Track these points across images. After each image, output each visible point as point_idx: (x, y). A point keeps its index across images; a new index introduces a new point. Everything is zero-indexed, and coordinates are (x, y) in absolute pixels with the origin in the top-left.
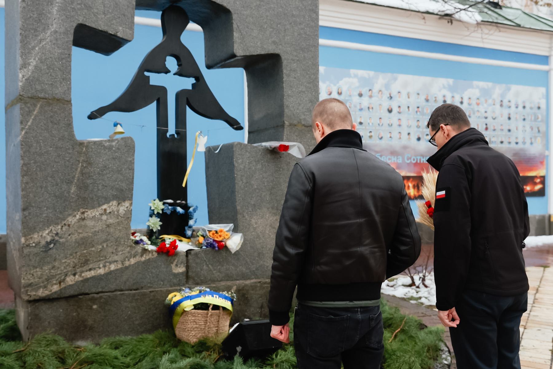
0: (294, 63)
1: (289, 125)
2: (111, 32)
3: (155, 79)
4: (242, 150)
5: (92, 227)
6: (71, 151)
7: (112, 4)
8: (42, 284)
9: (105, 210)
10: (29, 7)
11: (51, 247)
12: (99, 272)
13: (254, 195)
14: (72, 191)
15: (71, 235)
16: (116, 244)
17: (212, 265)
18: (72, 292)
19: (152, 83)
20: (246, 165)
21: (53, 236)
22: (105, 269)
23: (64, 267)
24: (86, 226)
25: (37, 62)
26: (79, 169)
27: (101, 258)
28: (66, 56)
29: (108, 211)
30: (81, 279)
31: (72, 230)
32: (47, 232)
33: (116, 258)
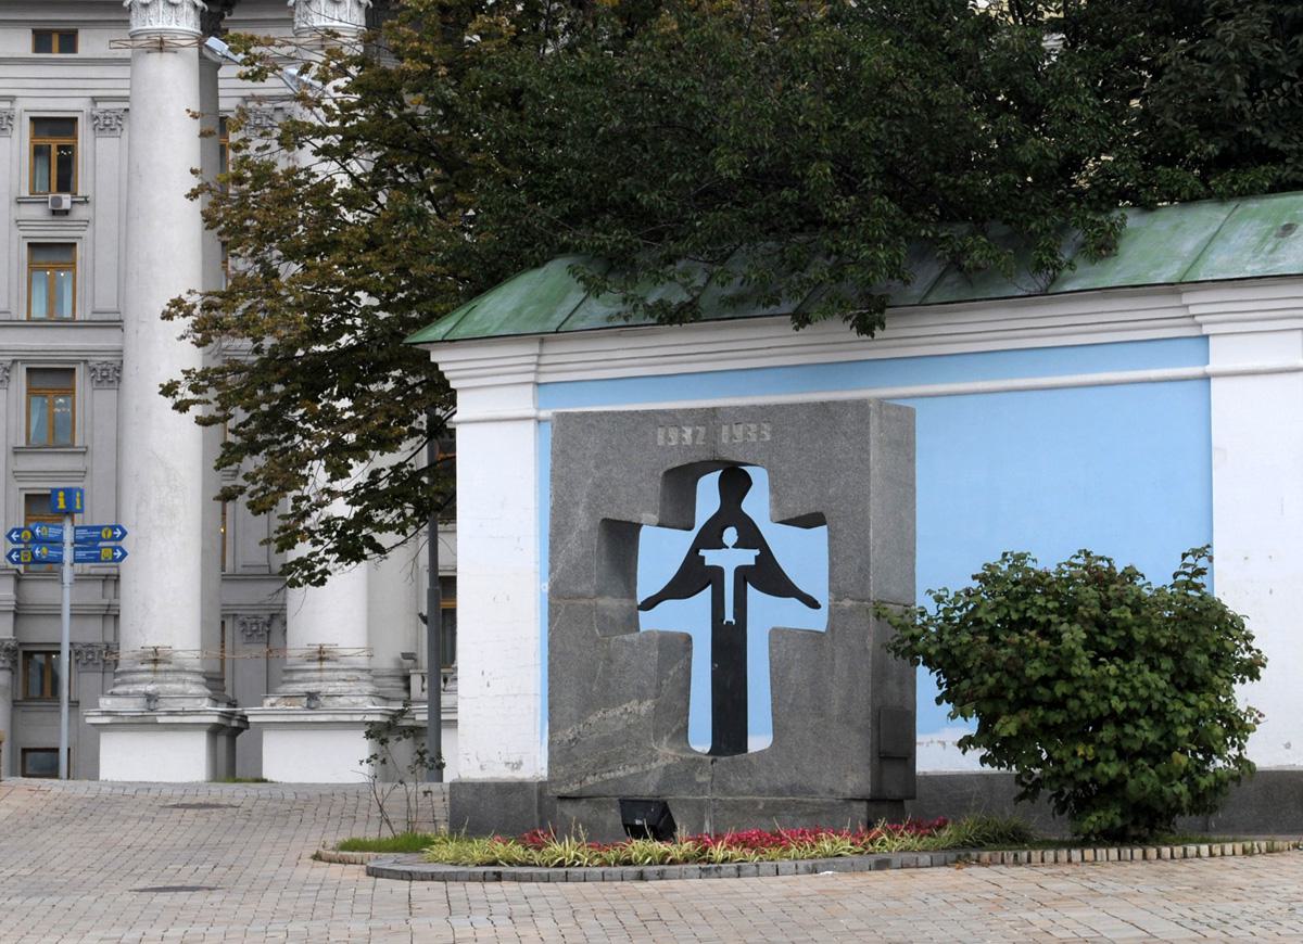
3: (711, 557)
18: (591, 793)
19: (706, 564)
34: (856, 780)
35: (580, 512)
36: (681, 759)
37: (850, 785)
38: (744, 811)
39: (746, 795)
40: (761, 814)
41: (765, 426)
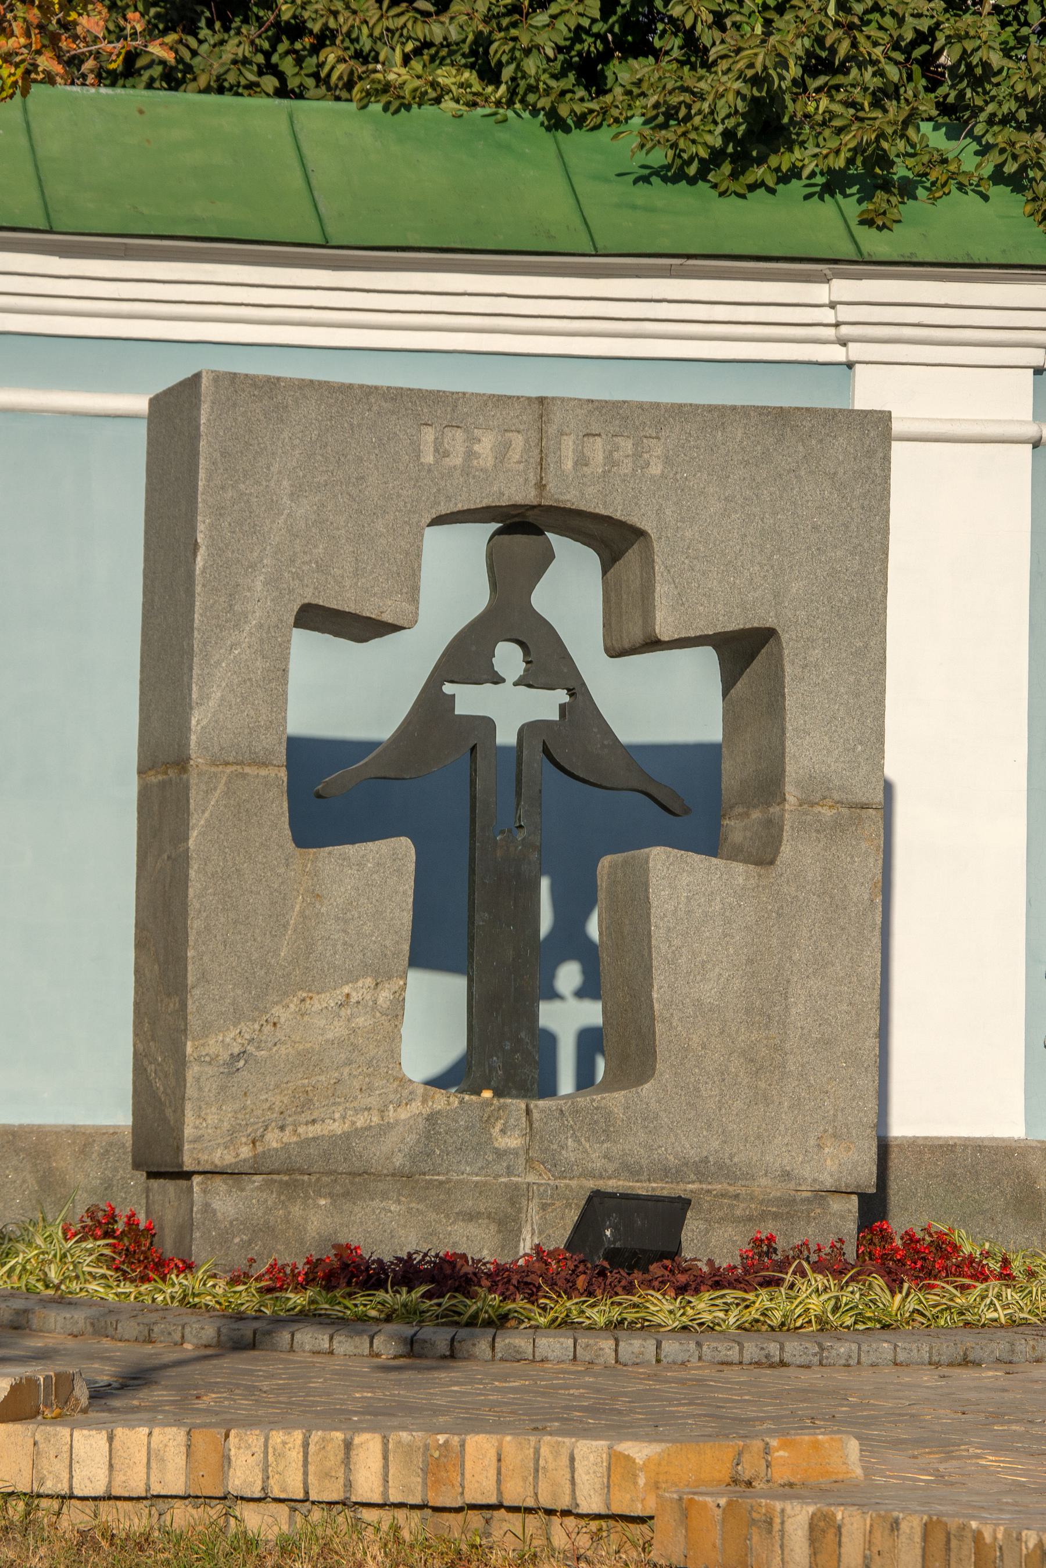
6: (282, 870)
8: (220, 1141)
9: (348, 995)
13: (699, 978)
15: (278, 1046)
17: (588, 1140)
19: (461, 709)
20: (679, 903)
21: (243, 1045)
26: (297, 908)
27: (338, 1100)
29: (353, 1000)
30: (295, 1139)
31: (280, 1035)
32: (232, 1036)
35: (259, 585)
39: (601, 1177)
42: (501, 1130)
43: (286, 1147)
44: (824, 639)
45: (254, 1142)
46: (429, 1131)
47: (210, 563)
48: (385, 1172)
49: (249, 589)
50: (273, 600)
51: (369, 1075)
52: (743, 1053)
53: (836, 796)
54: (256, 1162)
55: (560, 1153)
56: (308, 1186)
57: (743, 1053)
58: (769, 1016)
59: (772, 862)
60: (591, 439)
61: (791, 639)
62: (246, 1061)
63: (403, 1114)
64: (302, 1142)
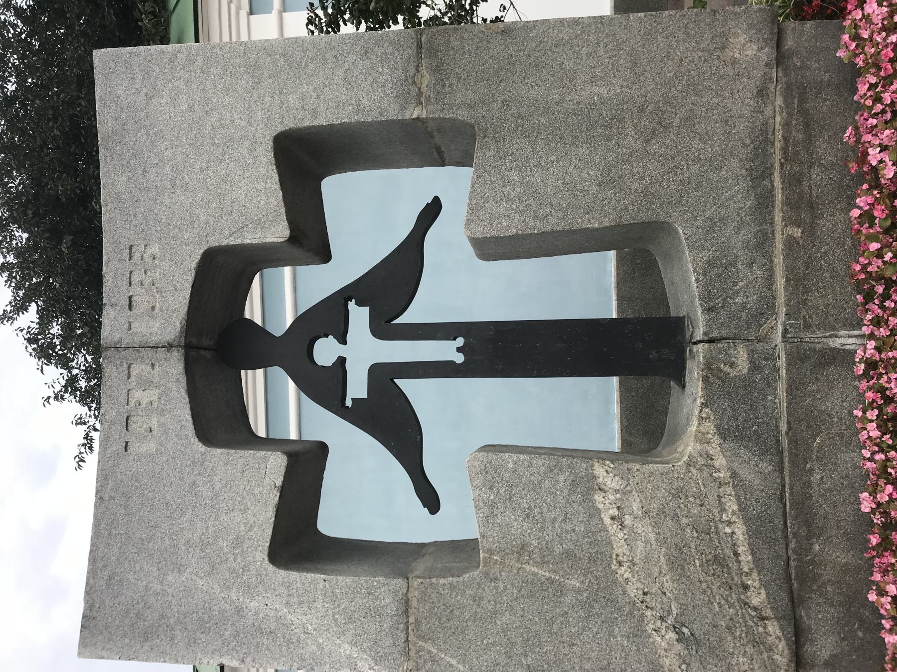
0: (288, 101)
1: (420, 106)
2: (277, 499)
4: (481, 218)
5: (649, 546)
7: (226, 495)
9: (613, 518)
10: (252, 651)
11: (689, 633)
12: (741, 538)
13: (579, 186)
14: (578, 585)
16: (683, 497)
22: (735, 522)
23: (729, 608)
24: (647, 560)
25: (343, 642)
26: (535, 569)
28: (327, 586)
29: (617, 513)
30: (755, 575)
31: (655, 589)
32: (659, 639)
33: (712, 498)
34: (742, 38)
35: (254, 604)
36: (704, 405)
37: (751, 51)
38: (807, 266)
40: (811, 232)
41: (137, 256)
42: (731, 366)
43: (765, 585)
44: (280, 94)
45: (763, 619)
46: (736, 436)
47: (235, 654)
48: (779, 480)
49: (257, 614)
50: (266, 591)
51: (687, 497)
52: (647, 141)
53: (412, 72)
54: (783, 618)
55: (750, 309)
56: (802, 561)
57: (647, 141)
58: (611, 119)
59: (472, 126)
60: (134, 304)
61: (282, 122)
62: (683, 625)
63: (720, 461)
64: (757, 566)
